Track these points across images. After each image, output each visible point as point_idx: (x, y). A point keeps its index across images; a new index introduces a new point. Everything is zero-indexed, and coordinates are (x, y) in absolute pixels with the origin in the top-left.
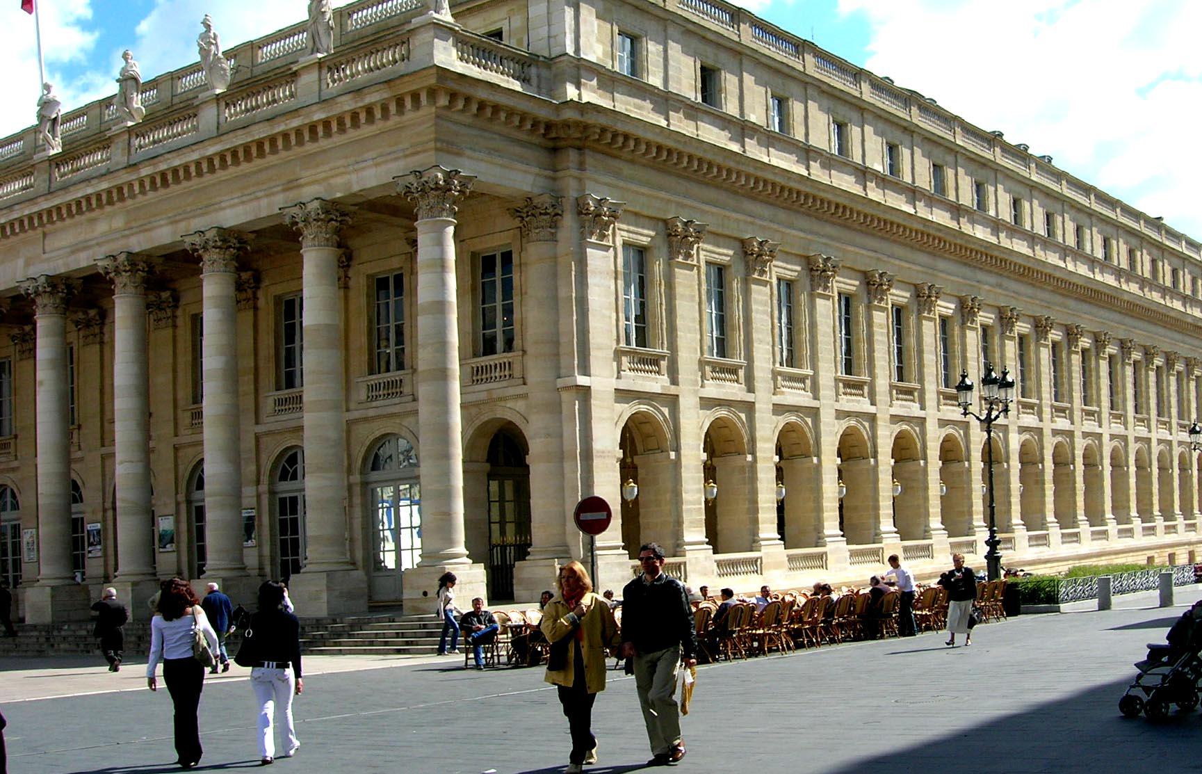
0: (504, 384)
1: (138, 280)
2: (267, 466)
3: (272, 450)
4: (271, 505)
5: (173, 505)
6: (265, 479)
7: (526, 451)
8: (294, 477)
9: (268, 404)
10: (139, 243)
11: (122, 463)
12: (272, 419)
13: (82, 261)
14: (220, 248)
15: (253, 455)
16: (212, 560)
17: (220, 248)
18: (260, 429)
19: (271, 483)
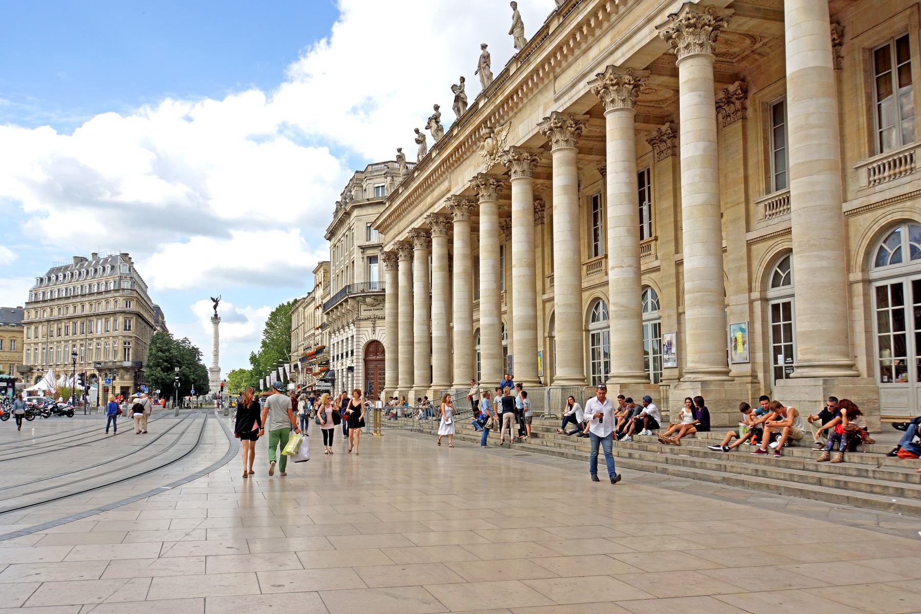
1: (625, 94)
2: (758, 271)
3: (764, 253)
4: (764, 312)
5: (675, 317)
6: (757, 285)
8: (787, 281)
9: (759, 211)
11: (613, 268)
12: (764, 224)
13: (582, 89)
14: (694, 26)
15: (745, 263)
17: (694, 26)
18: (752, 235)
19: (764, 290)
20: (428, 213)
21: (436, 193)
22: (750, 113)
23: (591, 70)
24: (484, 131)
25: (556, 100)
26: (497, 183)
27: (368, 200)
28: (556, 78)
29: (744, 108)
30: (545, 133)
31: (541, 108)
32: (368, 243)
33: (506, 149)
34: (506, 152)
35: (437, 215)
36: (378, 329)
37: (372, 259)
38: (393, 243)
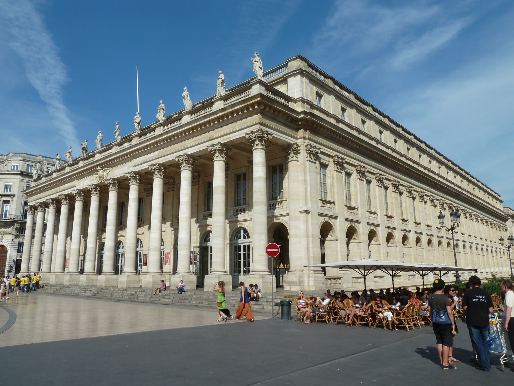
0: (280, 210)
7: (287, 233)
10: (161, 161)
13: (144, 166)
16: (180, 268)
20: (61, 193)
21: (67, 185)
22: (200, 183)
23: (149, 161)
24: (98, 168)
25: (133, 167)
26: (103, 190)
27: (8, 171)
29: (199, 182)
30: (128, 177)
31: (126, 167)
32: (4, 193)
33: (108, 178)
34: (108, 180)
36: (4, 239)
37: (7, 202)
38: (35, 202)
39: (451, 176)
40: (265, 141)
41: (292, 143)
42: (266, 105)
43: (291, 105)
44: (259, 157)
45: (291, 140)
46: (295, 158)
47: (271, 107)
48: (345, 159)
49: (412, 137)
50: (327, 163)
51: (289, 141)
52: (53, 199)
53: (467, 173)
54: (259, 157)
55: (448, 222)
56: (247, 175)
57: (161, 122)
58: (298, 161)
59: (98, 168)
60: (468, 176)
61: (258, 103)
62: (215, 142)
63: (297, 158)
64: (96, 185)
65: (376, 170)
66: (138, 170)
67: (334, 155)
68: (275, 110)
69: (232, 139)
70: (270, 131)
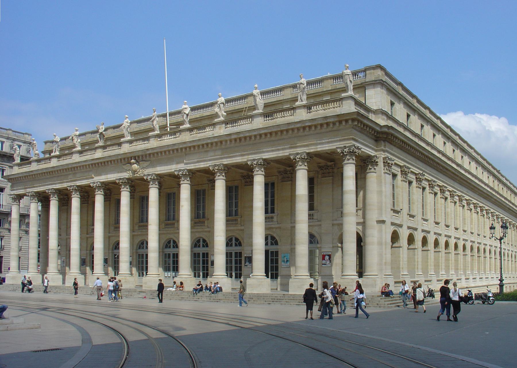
28: (186, 155)
35: (78, 186)
39: (485, 177)
40: (356, 156)
41: (373, 155)
42: (359, 121)
43: (372, 116)
44: (350, 171)
45: (372, 153)
46: (373, 170)
47: (361, 122)
48: (410, 168)
49: (457, 137)
50: (396, 172)
51: (370, 153)
52: (56, 190)
53: (498, 172)
54: (350, 171)
55: (499, 232)
56: (315, 180)
57: (222, 118)
58: (375, 172)
59: (133, 161)
60: (499, 175)
61: (353, 120)
62: (300, 150)
63: (375, 169)
64: (128, 179)
65: (430, 177)
66: (193, 168)
67: (402, 165)
68: (364, 125)
69: (319, 150)
70: (360, 146)
